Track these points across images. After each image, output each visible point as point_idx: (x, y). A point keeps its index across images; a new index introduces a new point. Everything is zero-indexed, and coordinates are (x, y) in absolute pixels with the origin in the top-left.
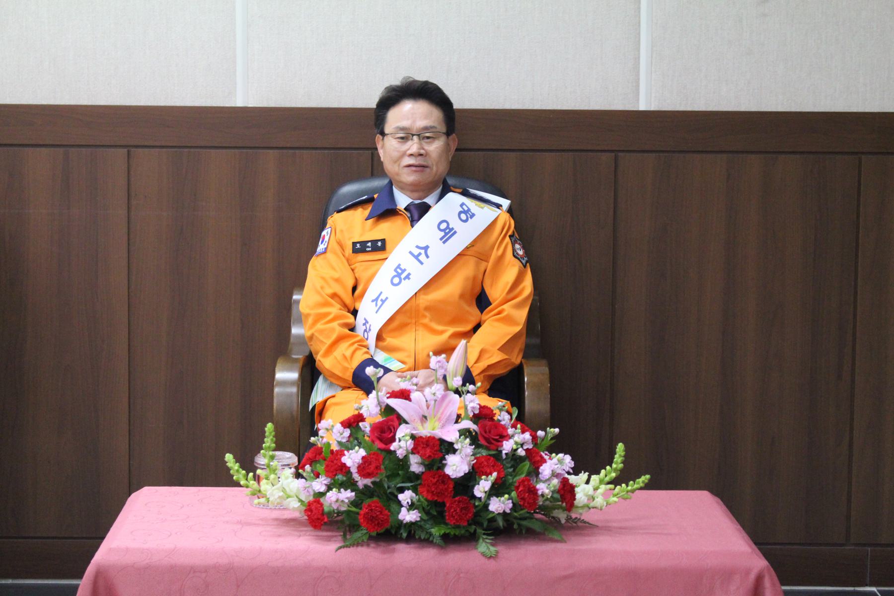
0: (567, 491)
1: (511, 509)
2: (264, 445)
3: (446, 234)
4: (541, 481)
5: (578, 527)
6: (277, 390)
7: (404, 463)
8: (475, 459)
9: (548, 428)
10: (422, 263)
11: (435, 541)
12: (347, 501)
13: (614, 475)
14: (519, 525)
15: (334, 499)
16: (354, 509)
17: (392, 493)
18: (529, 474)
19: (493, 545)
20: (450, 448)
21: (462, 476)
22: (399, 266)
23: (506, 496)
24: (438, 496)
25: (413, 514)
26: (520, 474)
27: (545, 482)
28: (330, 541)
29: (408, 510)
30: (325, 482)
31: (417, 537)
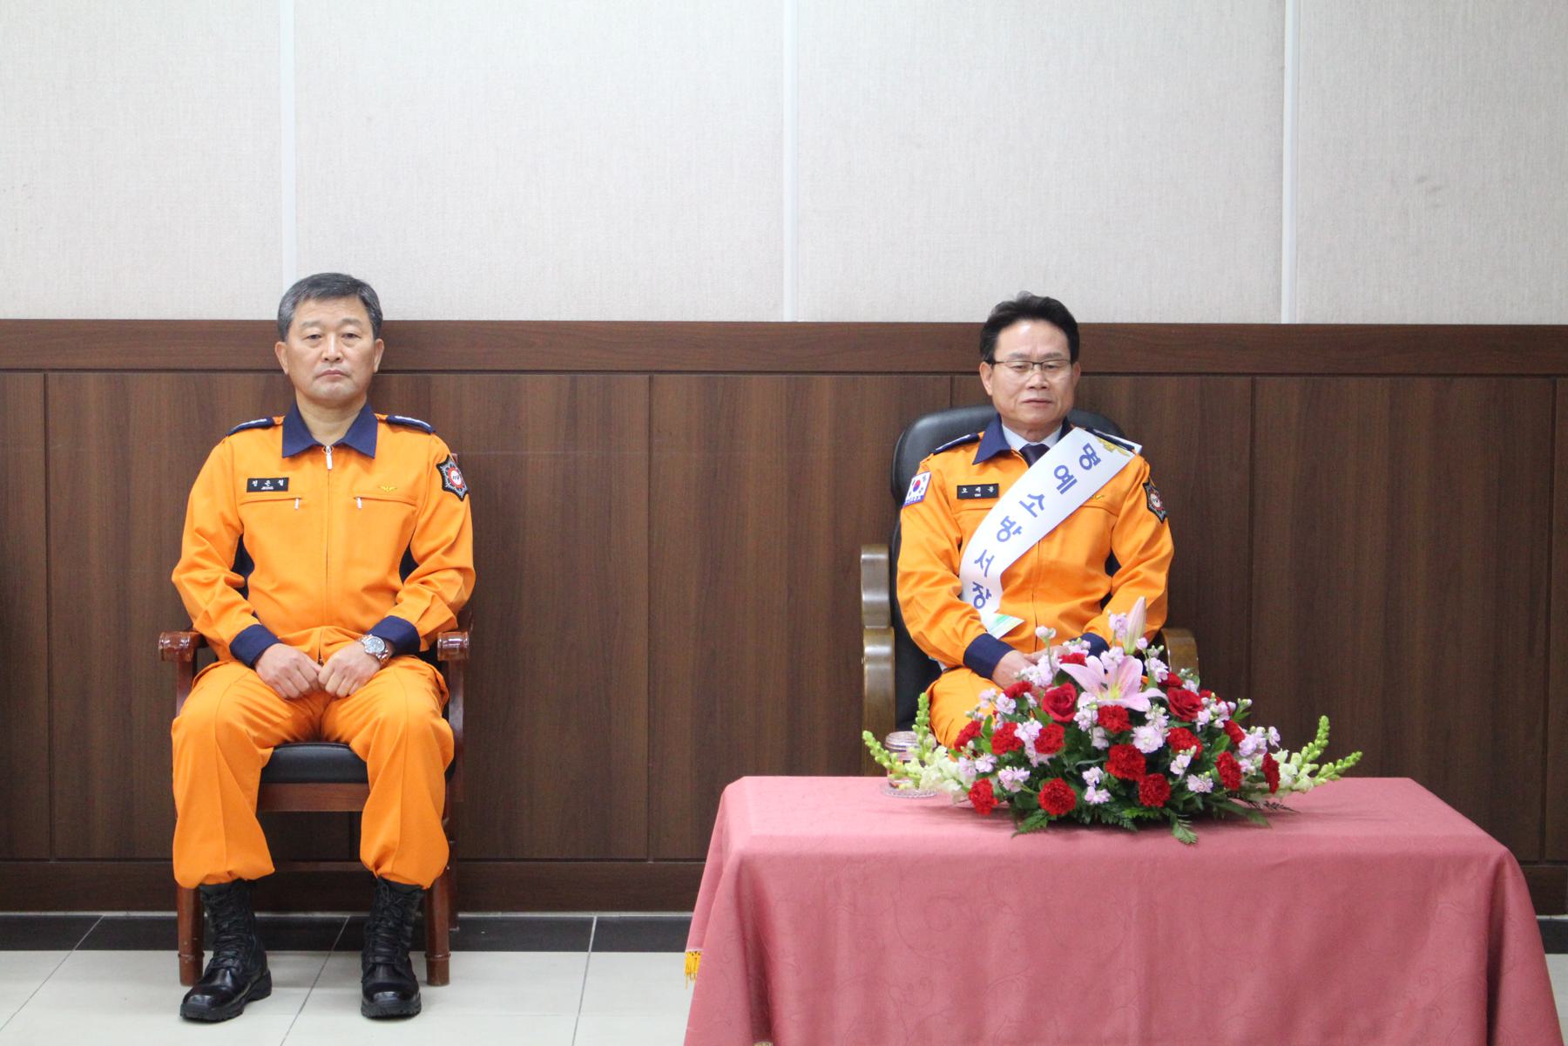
0: (1270, 770)
1: (1212, 789)
2: (917, 719)
3: (1065, 482)
4: (1241, 758)
5: (1276, 813)
6: (867, 667)
7: (1082, 738)
8: (1169, 731)
9: (1239, 699)
10: (1035, 515)
11: (1125, 826)
12: (1022, 781)
13: (1318, 752)
14: (1219, 808)
15: (1009, 777)
16: (1028, 790)
17: (1070, 773)
18: (1228, 748)
19: (1189, 829)
20: (1138, 718)
21: (1155, 752)
22: (1006, 519)
23: (1207, 773)
24: (1129, 774)
25: (1103, 794)
26: (1219, 749)
27: (1248, 757)
28: (999, 828)
29: (1096, 789)
30: (992, 761)
31: (1104, 822)
